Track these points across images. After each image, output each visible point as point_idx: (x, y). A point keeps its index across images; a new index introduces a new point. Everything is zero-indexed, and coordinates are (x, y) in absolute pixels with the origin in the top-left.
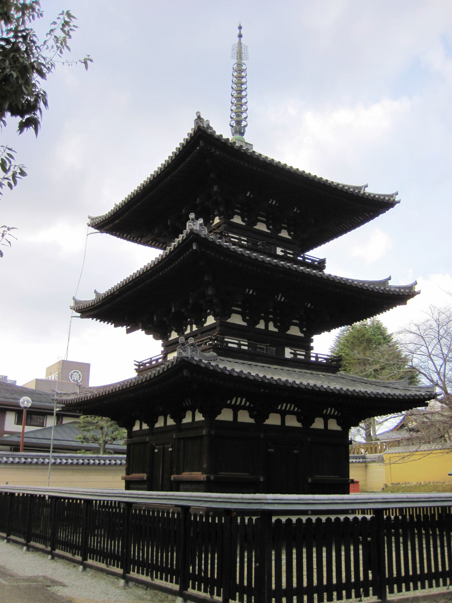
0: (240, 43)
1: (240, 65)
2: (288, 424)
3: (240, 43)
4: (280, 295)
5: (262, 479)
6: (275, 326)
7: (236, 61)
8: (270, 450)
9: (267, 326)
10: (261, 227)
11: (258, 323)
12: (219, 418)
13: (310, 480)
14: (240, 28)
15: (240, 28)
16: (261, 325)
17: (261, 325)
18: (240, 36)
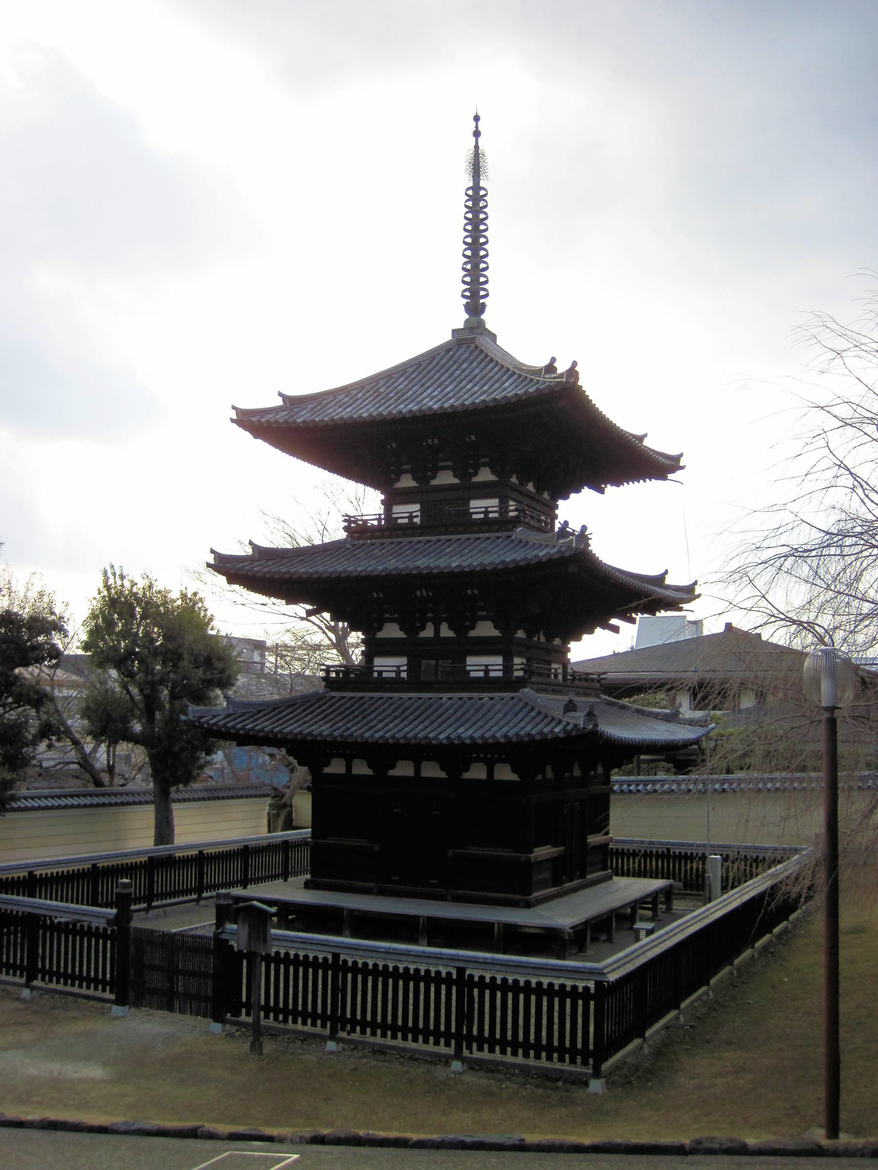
0: (477, 147)
1: (476, 187)
2: (424, 774)
3: (477, 147)
4: (424, 591)
5: (376, 848)
6: (450, 628)
7: (471, 184)
8: (395, 810)
9: (437, 631)
10: (446, 478)
11: (423, 628)
12: (327, 770)
13: (450, 853)
14: (477, 119)
15: (477, 119)
16: (428, 632)
17: (428, 632)
18: (477, 134)
